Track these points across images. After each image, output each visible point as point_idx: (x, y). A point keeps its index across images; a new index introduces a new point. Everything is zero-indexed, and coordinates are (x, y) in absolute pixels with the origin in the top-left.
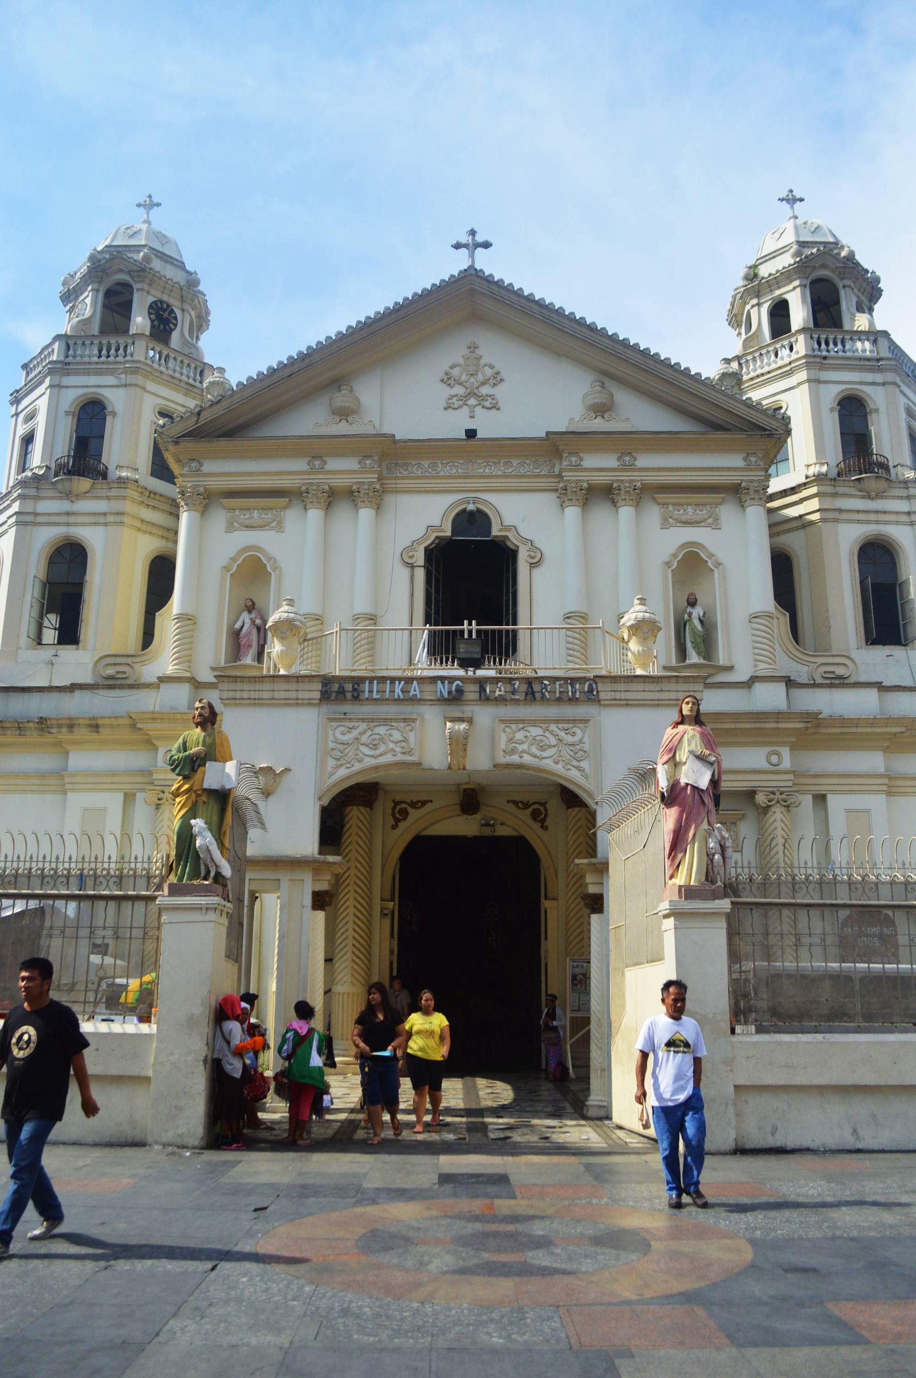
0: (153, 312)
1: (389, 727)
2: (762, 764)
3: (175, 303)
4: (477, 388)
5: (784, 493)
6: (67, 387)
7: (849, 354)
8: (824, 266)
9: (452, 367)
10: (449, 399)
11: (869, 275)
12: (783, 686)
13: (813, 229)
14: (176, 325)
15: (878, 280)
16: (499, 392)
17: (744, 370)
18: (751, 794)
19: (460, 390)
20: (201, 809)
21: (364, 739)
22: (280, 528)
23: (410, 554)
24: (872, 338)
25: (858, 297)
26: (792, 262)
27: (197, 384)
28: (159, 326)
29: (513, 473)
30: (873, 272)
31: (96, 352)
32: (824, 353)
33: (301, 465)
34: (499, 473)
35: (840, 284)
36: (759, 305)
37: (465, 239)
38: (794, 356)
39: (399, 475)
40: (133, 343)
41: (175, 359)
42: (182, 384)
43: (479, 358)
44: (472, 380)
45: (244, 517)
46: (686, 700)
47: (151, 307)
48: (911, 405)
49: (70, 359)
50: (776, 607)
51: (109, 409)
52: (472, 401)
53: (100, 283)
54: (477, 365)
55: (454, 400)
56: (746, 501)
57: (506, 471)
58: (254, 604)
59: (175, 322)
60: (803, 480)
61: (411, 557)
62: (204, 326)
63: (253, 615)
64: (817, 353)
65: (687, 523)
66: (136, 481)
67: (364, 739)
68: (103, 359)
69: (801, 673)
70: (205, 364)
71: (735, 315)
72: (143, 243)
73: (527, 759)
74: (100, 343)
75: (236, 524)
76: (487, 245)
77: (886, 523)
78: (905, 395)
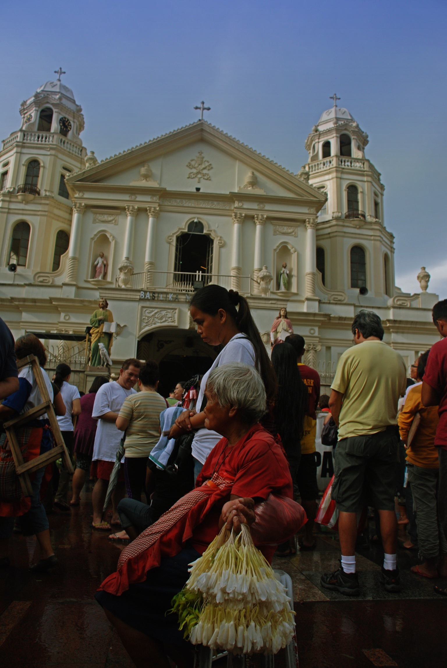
0: (61, 122)
1: (165, 312)
3: (71, 119)
4: (202, 170)
5: (324, 223)
6: (24, 153)
7: (353, 168)
8: (346, 129)
9: (192, 160)
10: (190, 174)
11: (364, 134)
12: (317, 303)
13: (343, 113)
14: (71, 129)
15: (367, 137)
17: (311, 170)
19: (195, 171)
20: (102, 339)
21: (157, 316)
22: (116, 224)
23: (170, 238)
24: (363, 162)
25: (359, 143)
26: (333, 126)
27: (79, 156)
28: (64, 129)
29: (215, 207)
30: (366, 133)
31: (36, 138)
32: (343, 167)
33: (126, 197)
34: (209, 207)
35: (352, 137)
36: (319, 142)
37: (200, 105)
38: (331, 167)
39: (167, 204)
40: (53, 137)
41: (70, 144)
42: (73, 156)
43: (203, 158)
44: (200, 167)
46: (282, 309)
47: (60, 120)
48: (377, 191)
49: (25, 141)
50: (317, 271)
51: (42, 164)
52: (199, 176)
53: (39, 107)
54: (202, 161)
55: (192, 174)
56: (308, 227)
57: (212, 206)
58: (103, 255)
59: (70, 127)
60: (331, 218)
61: (171, 239)
62: (82, 129)
64: (341, 166)
65: (284, 234)
66: (53, 197)
68: (40, 142)
69: (325, 298)
70: (83, 148)
71: (309, 145)
72: (58, 90)
74: (49, 142)
75: (97, 220)
76: (209, 109)
77: (362, 239)
78: (374, 186)
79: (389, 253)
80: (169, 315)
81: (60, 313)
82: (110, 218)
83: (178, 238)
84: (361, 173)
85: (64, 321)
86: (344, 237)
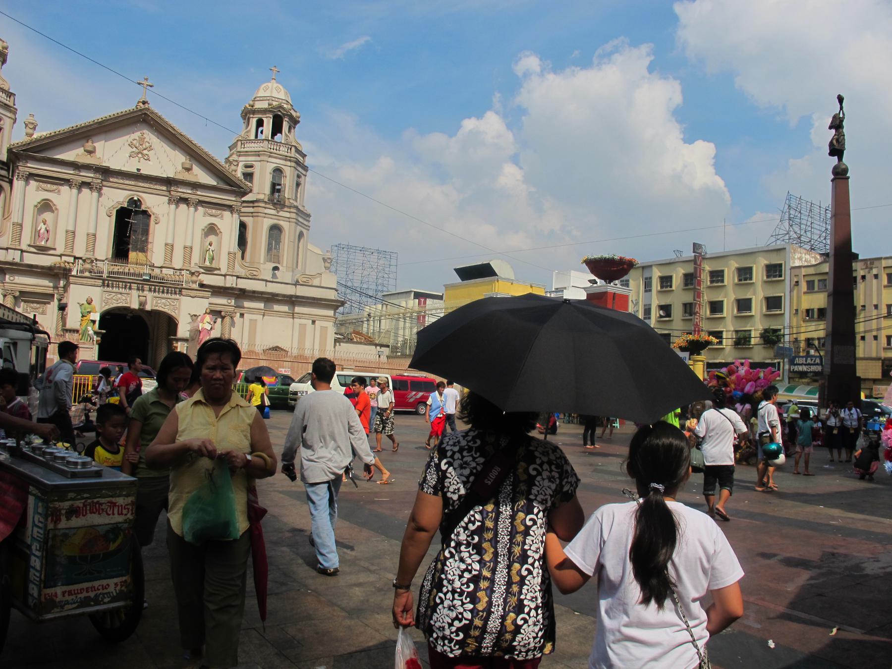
2: (226, 303)
8: (280, 111)
9: (133, 140)
16: (151, 153)
18: (220, 312)
19: (134, 149)
21: (114, 298)
24: (290, 147)
45: (44, 185)
52: (140, 155)
63: (45, 226)
67: (114, 298)
73: (161, 309)
77: (279, 220)
79: (305, 231)
80: (124, 298)
81: (5, 274)
82: (55, 187)
83: (117, 211)
84: (286, 158)
85: (9, 281)
86: (265, 217)
